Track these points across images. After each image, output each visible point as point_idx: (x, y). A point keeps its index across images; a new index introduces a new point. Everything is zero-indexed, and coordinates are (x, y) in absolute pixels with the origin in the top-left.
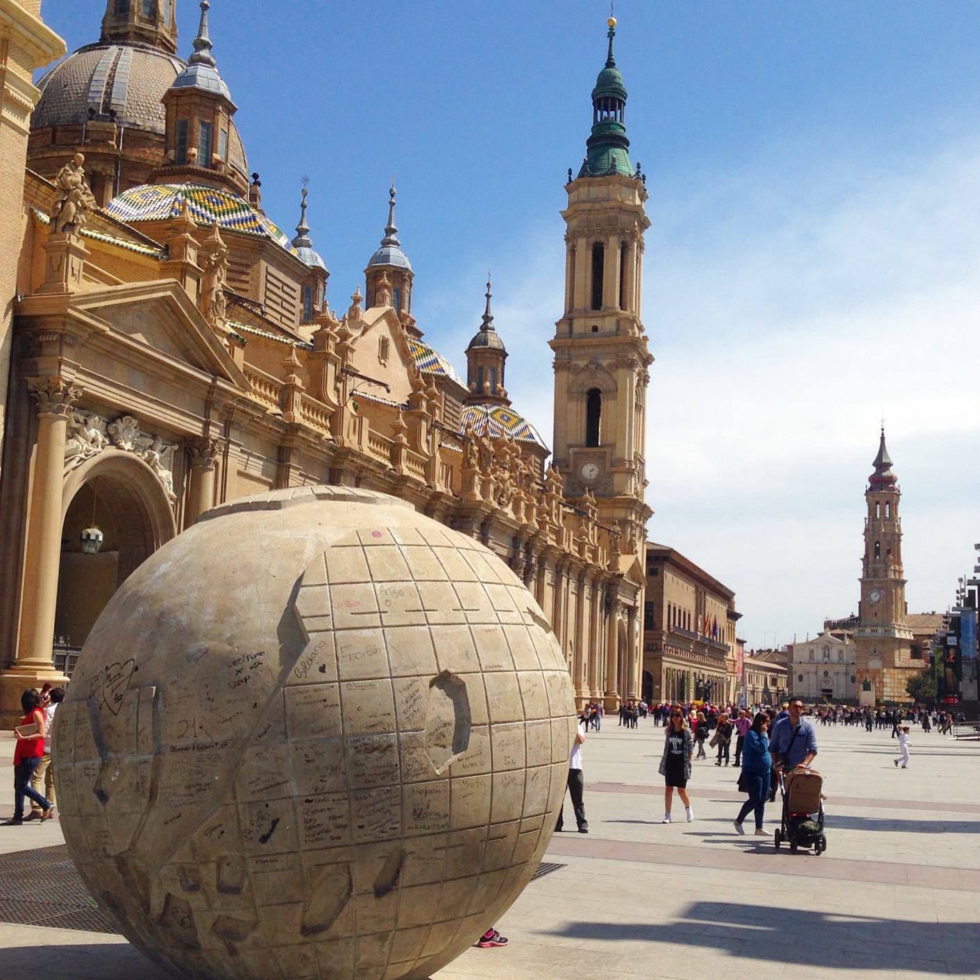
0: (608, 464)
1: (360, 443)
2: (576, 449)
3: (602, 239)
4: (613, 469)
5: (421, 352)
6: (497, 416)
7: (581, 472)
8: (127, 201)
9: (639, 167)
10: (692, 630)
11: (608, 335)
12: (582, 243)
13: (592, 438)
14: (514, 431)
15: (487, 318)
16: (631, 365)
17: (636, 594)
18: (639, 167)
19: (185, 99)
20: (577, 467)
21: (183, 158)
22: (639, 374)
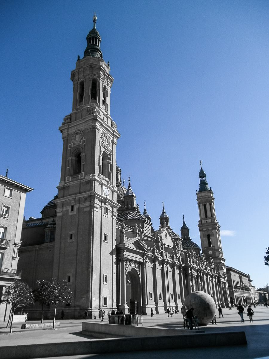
0: (214, 250)
2: (206, 248)
3: (206, 203)
5: (173, 233)
7: (209, 254)
9: (211, 188)
10: (240, 286)
11: (210, 223)
12: (201, 205)
14: (193, 246)
15: (184, 222)
17: (225, 279)
18: (211, 188)
20: (208, 252)
21: (128, 207)
22: (218, 230)
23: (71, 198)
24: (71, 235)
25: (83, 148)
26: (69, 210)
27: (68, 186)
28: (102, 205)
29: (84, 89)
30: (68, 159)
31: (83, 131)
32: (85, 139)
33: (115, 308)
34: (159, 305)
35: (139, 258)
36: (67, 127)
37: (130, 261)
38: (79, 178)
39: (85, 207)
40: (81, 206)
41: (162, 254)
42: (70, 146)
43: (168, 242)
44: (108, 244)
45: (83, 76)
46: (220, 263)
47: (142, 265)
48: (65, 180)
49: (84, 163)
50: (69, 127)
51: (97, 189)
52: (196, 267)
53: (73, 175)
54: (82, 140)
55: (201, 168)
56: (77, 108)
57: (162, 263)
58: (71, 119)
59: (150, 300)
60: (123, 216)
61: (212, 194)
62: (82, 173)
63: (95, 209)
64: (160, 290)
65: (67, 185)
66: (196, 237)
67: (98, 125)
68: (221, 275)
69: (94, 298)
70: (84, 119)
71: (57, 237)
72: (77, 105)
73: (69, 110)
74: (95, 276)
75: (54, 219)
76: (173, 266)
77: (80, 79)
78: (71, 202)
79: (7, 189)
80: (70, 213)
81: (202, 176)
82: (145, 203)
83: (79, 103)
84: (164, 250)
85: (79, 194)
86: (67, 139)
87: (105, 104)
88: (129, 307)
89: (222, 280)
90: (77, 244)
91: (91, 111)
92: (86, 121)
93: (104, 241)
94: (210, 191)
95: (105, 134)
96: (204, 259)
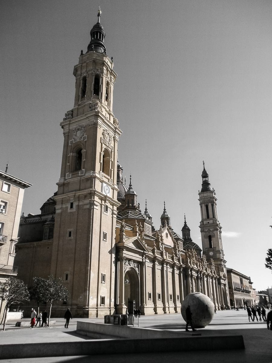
0: (215, 252)
1: (166, 257)
2: (207, 249)
3: (208, 204)
4: (216, 253)
6: (190, 244)
7: (209, 255)
10: (240, 288)
11: (212, 224)
12: (203, 205)
15: (185, 223)
19: (128, 196)
20: (208, 253)
21: (129, 206)
22: (219, 231)
23: (71, 194)
24: (70, 233)
25: (84, 144)
26: (68, 207)
27: (68, 183)
28: (102, 202)
29: (87, 85)
30: (69, 155)
31: (84, 127)
32: (86, 136)
33: (113, 307)
34: (157, 306)
35: (138, 258)
36: (69, 123)
37: (130, 260)
38: (80, 175)
39: (85, 205)
40: (81, 203)
41: (162, 254)
42: (70, 142)
43: (168, 242)
44: (107, 243)
45: (86, 71)
46: (221, 265)
47: (141, 264)
48: (65, 176)
49: (85, 160)
50: (71, 122)
51: (98, 186)
52: (196, 267)
53: (73, 171)
54: (84, 136)
55: (204, 168)
56: (79, 103)
57: (162, 263)
58: (72, 115)
59: (149, 300)
60: (123, 214)
61: (215, 194)
62: (83, 169)
63: (95, 207)
64: (159, 290)
65: (67, 181)
66: (197, 238)
67: (100, 121)
68: (221, 277)
69: (92, 297)
70: (86, 115)
71: (56, 234)
72: (79, 101)
73: (71, 105)
74: (93, 275)
75: (53, 216)
76: (173, 266)
77: (82, 75)
78: (71, 199)
79: (5, 183)
80: (69, 210)
81: (204, 176)
82: (146, 202)
83: (81, 98)
84: (164, 250)
85: (79, 191)
86: (68, 135)
87: (108, 100)
88: (127, 307)
89: (222, 281)
90: (76, 242)
91: (93, 106)
92: (89, 117)
93: (103, 240)
94: (213, 192)
95: (107, 130)
96: (205, 260)
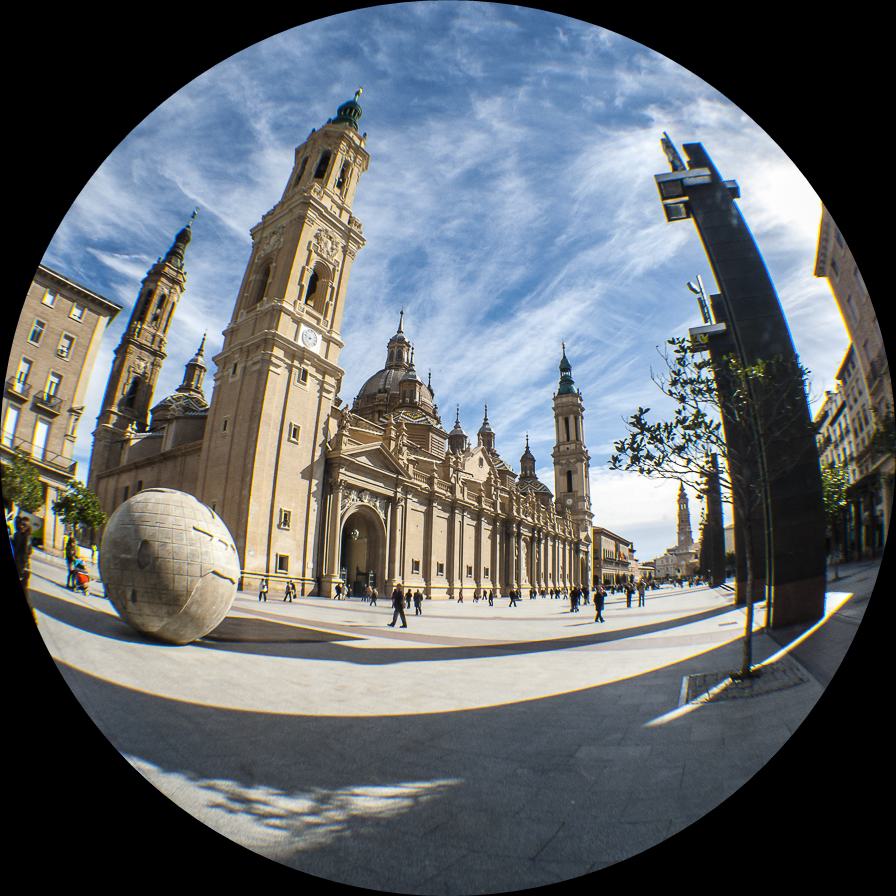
8: (384, 418)
12: (560, 418)
13: (570, 489)
15: (527, 448)
16: (582, 461)
20: (565, 501)
37: (361, 491)
43: (476, 470)
46: (583, 520)
47: (390, 502)
51: (285, 328)
52: (531, 520)
57: (452, 507)
61: (581, 400)
63: (272, 368)
64: (439, 555)
66: (547, 477)
67: (311, 213)
69: (252, 553)
74: (257, 508)
76: (478, 516)
89: (582, 548)
90: (232, 440)
93: (289, 440)
94: (578, 395)
